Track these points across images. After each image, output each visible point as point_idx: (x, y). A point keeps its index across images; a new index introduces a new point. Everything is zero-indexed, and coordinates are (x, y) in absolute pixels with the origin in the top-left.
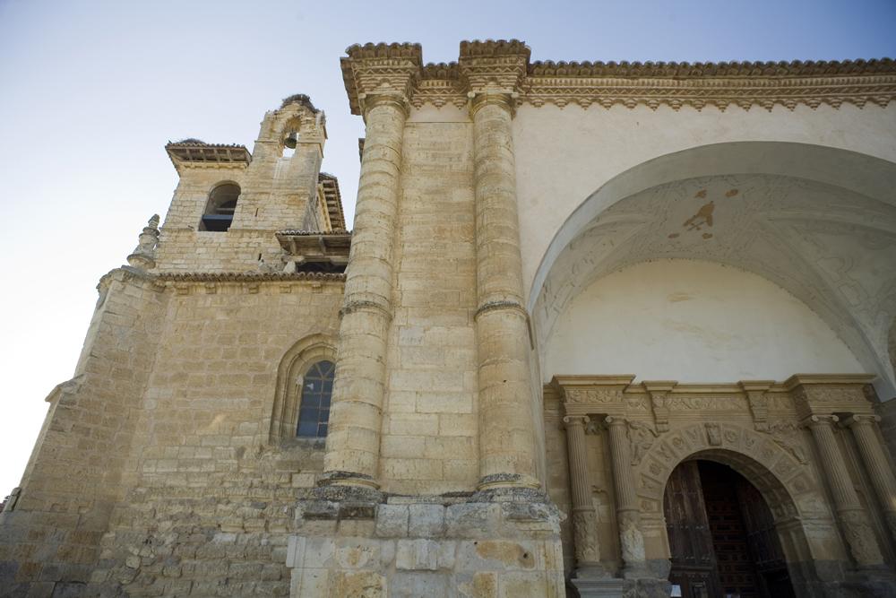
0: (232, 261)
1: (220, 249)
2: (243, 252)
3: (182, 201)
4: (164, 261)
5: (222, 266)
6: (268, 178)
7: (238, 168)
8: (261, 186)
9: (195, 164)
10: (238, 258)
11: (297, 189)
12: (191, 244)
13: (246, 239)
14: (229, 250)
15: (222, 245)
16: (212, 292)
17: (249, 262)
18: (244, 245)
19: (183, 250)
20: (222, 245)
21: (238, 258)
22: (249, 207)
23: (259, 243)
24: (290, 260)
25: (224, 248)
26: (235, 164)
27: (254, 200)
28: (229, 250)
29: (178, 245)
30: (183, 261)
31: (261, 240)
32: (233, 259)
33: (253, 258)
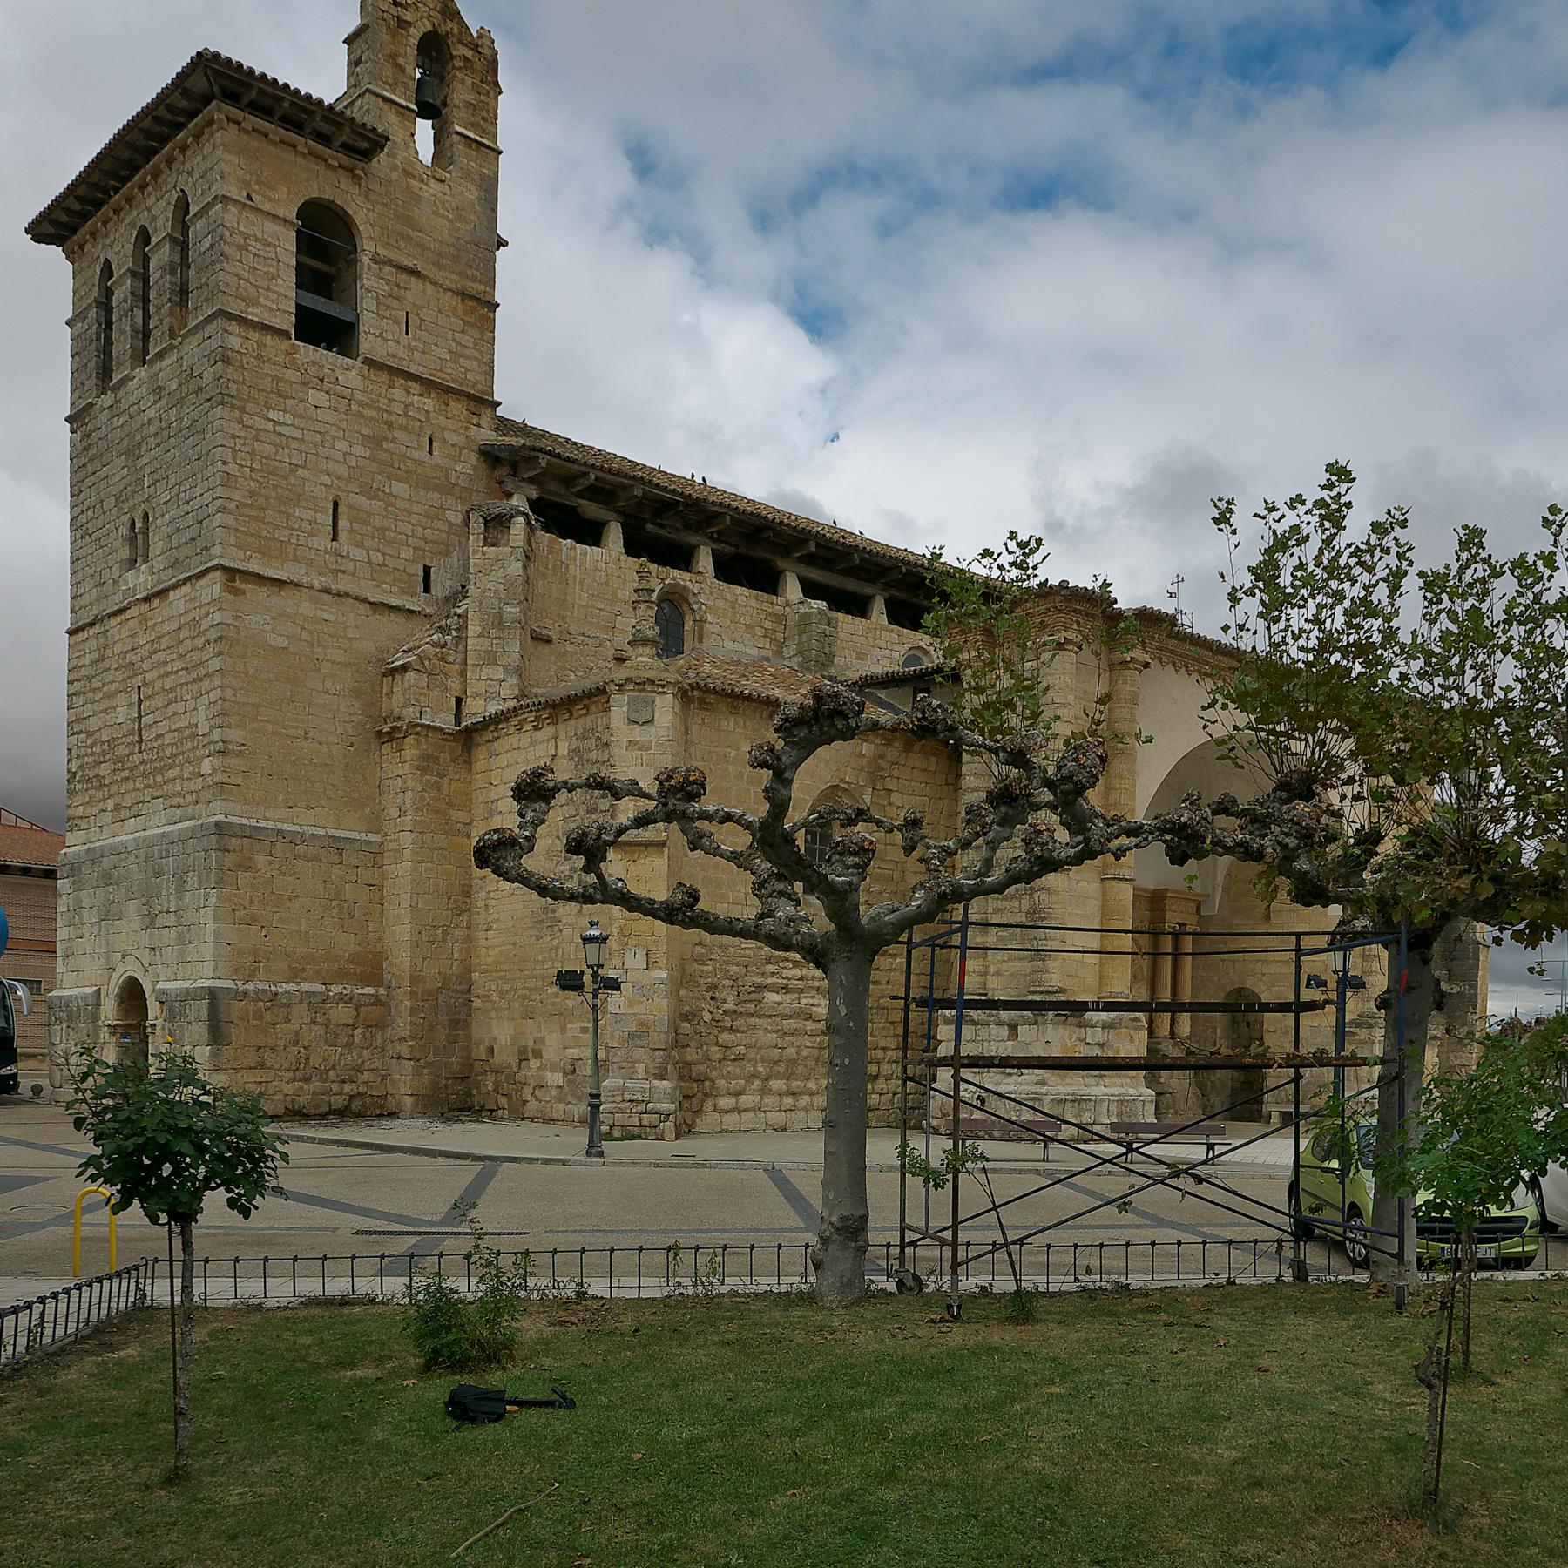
0: (385, 444)
1: (354, 407)
2: (402, 428)
3: (246, 236)
4: (250, 407)
5: (367, 454)
6: (410, 222)
7: (351, 170)
8: (402, 244)
9: (252, 121)
10: (394, 440)
11: (474, 279)
12: (291, 375)
13: (398, 393)
14: (373, 413)
15: (359, 396)
16: (734, 710)
17: (415, 454)
18: (398, 408)
19: (282, 387)
20: (359, 396)
21: (394, 440)
22: (389, 301)
23: (427, 412)
24: (518, 489)
25: (361, 404)
26: (347, 161)
27: (398, 286)
28: (373, 413)
29: (267, 368)
30: (288, 419)
31: (429, 403)
32: (386, 439)
33: (419, 448)
